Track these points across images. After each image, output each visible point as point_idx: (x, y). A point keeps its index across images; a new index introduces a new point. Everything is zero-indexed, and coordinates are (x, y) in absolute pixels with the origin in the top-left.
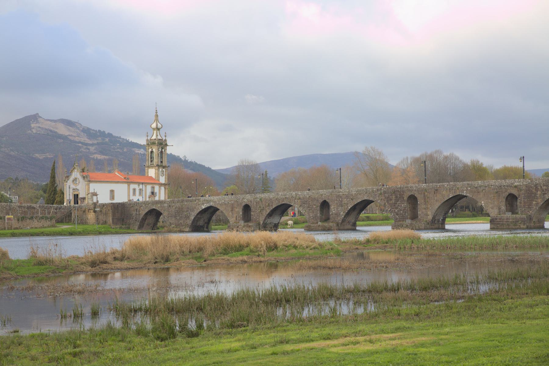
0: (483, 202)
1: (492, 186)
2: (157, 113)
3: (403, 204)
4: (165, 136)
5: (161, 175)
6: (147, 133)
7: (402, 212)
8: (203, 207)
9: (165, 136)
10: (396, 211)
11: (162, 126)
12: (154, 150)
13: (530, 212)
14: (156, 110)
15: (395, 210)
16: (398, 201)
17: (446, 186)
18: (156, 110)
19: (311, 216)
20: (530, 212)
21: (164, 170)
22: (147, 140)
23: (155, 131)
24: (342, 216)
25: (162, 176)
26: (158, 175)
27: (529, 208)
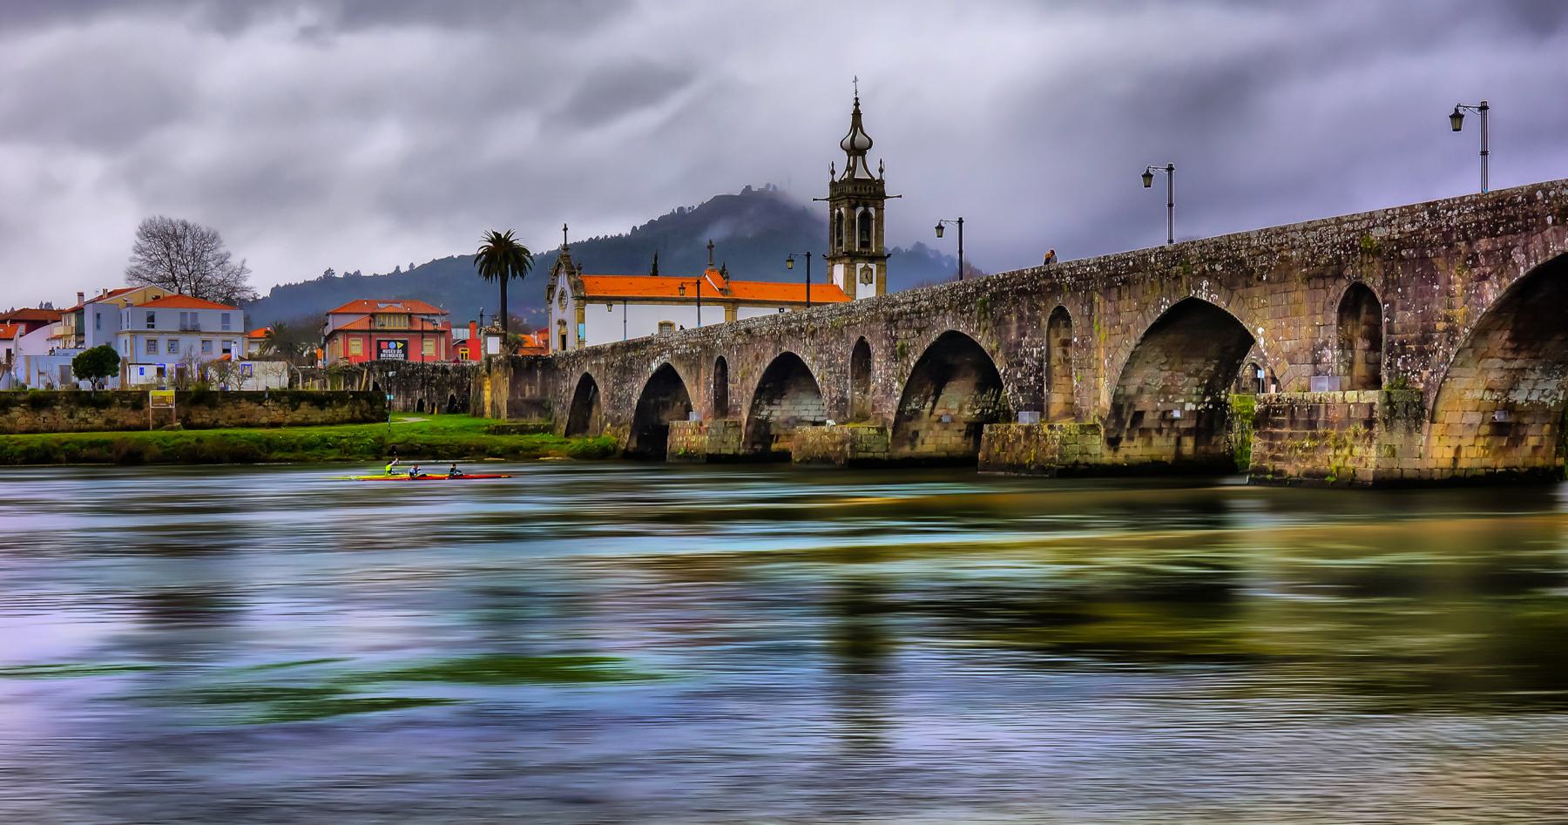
0: (1260, 330)
1: (1293, 248)
2: (857, 104)
3: (1037, 346)
4: (881, 170)
5: (861, 282)
6: (833, 164)
7: (1032, 379)
8: (655, 366)
9: (881, 170)
10: (1019, 376)
11: (871, 142)
12: (842, 209)
13: (1426, 374)
14: (857, 99)
15: (1016, 374)
16: (1024, 335)
17: (1153, 260)
18: (857, 99)
19: (834, 395)
20: (1426, 374)
21: (873, 266)
22: (833, 184)
23: (851, 158)
24: (895, 396)
25: (866, 285)
26: (850, 279)
27: (1421, 352)
